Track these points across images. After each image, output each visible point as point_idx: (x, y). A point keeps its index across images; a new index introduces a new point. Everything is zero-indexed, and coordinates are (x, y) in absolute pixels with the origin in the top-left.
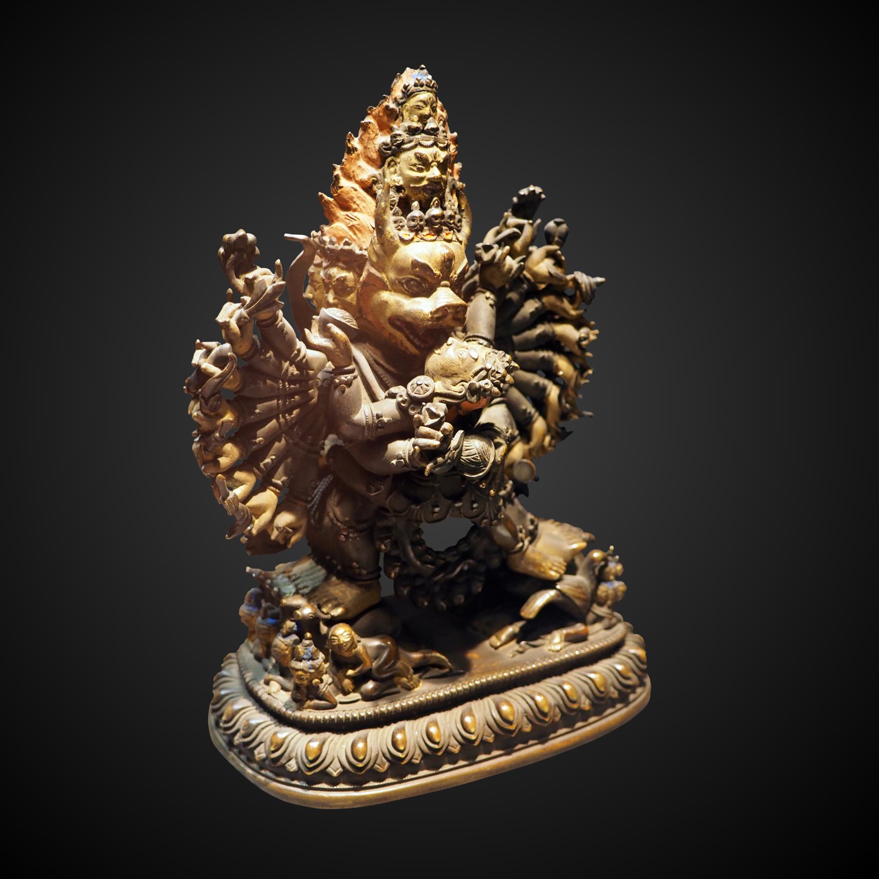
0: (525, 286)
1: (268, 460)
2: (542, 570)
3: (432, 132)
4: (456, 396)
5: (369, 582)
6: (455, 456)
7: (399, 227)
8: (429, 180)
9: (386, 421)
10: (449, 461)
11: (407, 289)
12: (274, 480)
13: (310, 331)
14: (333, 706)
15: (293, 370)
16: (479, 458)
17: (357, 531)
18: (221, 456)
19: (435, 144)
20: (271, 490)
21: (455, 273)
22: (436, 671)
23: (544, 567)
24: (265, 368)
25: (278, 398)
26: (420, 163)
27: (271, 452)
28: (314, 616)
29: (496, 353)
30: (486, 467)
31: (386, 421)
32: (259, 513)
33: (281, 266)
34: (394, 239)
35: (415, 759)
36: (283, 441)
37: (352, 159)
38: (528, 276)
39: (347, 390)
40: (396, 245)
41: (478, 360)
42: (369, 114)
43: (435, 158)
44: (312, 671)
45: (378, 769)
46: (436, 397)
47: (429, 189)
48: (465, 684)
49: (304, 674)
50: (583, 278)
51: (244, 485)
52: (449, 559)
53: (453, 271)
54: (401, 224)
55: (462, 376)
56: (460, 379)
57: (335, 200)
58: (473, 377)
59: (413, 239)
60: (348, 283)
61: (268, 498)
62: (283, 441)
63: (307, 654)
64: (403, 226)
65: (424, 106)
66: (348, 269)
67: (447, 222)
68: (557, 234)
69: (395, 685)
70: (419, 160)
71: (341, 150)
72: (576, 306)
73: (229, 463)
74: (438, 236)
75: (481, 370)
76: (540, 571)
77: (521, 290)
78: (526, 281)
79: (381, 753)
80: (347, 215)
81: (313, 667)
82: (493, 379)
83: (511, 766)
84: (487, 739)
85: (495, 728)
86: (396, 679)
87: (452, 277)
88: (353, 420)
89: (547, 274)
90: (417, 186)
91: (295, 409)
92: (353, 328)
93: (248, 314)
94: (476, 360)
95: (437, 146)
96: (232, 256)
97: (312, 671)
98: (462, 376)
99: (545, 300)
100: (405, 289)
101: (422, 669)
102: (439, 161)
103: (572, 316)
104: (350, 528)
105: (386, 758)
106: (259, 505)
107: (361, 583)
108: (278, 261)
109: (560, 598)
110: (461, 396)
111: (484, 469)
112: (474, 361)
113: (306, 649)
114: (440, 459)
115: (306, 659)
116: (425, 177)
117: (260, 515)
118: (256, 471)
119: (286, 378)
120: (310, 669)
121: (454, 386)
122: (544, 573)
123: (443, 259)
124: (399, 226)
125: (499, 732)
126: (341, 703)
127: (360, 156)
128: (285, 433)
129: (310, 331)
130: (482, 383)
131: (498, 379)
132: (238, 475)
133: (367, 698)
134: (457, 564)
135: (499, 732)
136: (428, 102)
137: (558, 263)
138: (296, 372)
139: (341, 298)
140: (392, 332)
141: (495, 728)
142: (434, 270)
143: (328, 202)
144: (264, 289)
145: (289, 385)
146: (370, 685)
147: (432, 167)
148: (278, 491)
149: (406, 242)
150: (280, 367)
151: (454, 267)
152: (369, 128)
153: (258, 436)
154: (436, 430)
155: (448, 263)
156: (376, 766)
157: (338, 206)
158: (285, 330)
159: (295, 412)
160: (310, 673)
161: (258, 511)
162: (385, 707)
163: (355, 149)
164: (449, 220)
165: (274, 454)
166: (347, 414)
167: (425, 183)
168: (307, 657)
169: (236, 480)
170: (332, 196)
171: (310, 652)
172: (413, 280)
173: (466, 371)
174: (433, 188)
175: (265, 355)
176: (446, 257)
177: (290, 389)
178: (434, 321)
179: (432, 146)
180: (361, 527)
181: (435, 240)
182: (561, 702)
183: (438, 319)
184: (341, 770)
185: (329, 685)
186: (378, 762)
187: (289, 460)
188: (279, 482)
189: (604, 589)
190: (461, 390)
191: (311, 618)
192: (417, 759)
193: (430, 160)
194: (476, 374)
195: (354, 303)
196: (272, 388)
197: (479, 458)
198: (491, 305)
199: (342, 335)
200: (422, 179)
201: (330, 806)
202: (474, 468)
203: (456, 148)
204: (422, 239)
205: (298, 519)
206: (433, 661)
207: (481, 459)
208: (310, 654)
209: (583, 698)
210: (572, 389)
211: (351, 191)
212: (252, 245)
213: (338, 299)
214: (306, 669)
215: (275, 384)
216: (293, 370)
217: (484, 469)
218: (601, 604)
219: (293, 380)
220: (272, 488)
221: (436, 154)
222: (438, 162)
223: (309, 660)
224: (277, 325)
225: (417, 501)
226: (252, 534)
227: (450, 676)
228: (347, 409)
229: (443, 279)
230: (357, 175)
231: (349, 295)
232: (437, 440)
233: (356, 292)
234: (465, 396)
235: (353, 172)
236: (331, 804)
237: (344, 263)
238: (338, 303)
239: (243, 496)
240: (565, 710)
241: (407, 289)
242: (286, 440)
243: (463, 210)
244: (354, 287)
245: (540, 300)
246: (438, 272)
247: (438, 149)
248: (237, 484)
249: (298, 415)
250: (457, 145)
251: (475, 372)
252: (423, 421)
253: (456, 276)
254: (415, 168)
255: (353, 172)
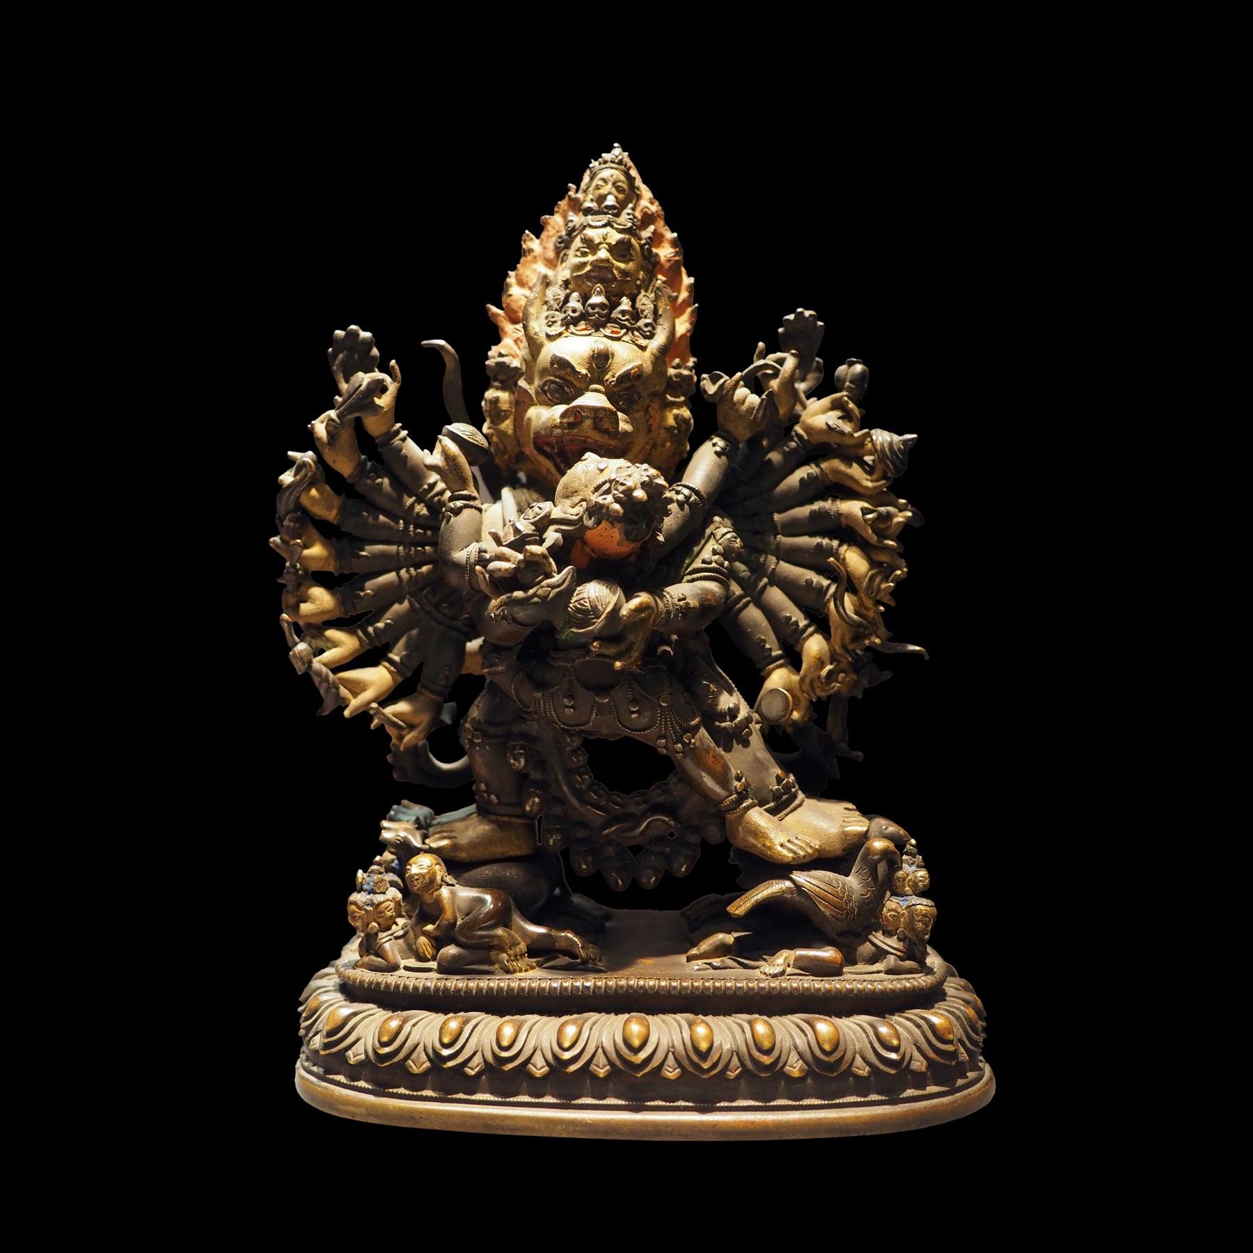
0: (793, 444)
1: (380, 625)
2: (768, 844)
3: (606, 210)
4: (571, 520)
5: (506, 819)
6: (551, 596)
7: (550, 323)
8: (592, 263)
9: (488, 558)
10: (536, 599)
11: (551, 398)
12: (391, 655)
13: (432, 454)
14: (394, 968)
15: (421, 509)
16: (588, 604)
17: (485, 735)
18: (305, 602)
19: (609, 224)
20: (385, 667)
21: (613, 376)
22: (564, 960)
23: (771, 840)
24: (381, 501)
25: (399, 544)
26: (585, 245)
27: (388, 615)
28: (402, 841)
29: (638, 467)
30: (598, 618)
31: (488, 558)
32: (359, 692)
33: (379, 360)
34: (538, 336)
35: (468, 1067)
36: (406, 603)
37: (526, 262)
38: (801, 432)
39: (452, 519)
40: (541, 343)
41: (604, 472)
42: (557, 212)
43: (605, 239)
44: (369, 908)
45: (411, 1067)
46: (552, 525)
47: (594, 277)
48: (587, 981)
49: (357, 910)
50: (881, 437)
51: (338, 648)
52: (632, 809)
53: (610, 373)
54: (552, 320)
55: (582, 493)
56: (579, 498)
57: (506, 313)
58: (593, 494)
59: (560, 334)
60: (501, 405)
61: (377, 677)
62: (406, 603)
63: (368, 884)
64: (556, 322)
65: (604, 184)
66: (503, 389)
67: (617, 318)
68: (849, 377)
69: (492, 963)
70: (584, 243)
71: (513, 256)
72: (875, 477)
73: (314, 611)
74: (596, 331)
75: (604, 483)
76: (764, 845)
77: (787, 449)
78: (796, 439)
79: (421, 1046)
80: (516, 329)
81: (372, 904)
82: (616, 492)
83: (632, 1133)
84: (595, 1070)
85: (613, 1056)
86: (493, 954)
87: (607, 380)
88: (453, 557)
89: (824, 426)
90: (579, 273)
91: (426, 564)
92: (469, 442)
93: (338, 416)
94: (602, 471)
95: (612, 227)
96: (341, 356)
97: (369, 908)
98: (582, 493)
99: (824, 465)
100: (549, 399)
101: (541, 952)
102: (610, 243)
103: (867, 488)
104: (476, 730)
105: (427, 1055)
106: (357, 679)
107: (494, 817)
108: (393, 362)
109: (796, 897)
110: (576, 520)
111: (595, 620)
112: (598, 472)
113: (369, 876)
114: (518, 594)
115: (366, 890)
116: (588, 261)
117: (359, 694)
118: (360, 633)
119: (408, 515)
120: (368, 905)
121: (573, 507)
122: (770, 848)
123: (591, 354)
124: (549, 321)
125: (618, 1063)
126: (407, 968)
127: (538, 258)
128: (411, 595)
129: (432, 454)
130: (600, 500)
131: (621, 493)
132: (332, 633)
133: (447, 969)
134: (644, 816)
135: (618, 1063)
136: (609, 180)
137: (847, 416)
138: (425, 511)
139: (496, 427)
140: (549, 468)
141: (613, 1056)
142: (576, 366)
143: (499, 315)
144: (357, 385)
145: (415, 528)
146: (451, 950)
147: (600, 250)
148: (392, 668)
149: (550, 338)
150: (400, 501)
151: (612, 368)
152: (549, 224)
153: (366, 588)
154: (516, 551)
155: (601, 360)
156: (410, 1062)
157: (508, 319)
158: (404, 451)
159: (424, 569)
160: (366, 910)
161: (356, 687)
162: (455, 983)
163: (531, 251)
164: (620, 316)
165: (390, 617)
166: (447, 549)
167: (588, 268)
168: (367, 888)
169: (328, 640)
170: (502, 308)
171: (372, 881)
172: (553, 382)
173: (586, 487)
174: (599, 276)
175: (374, 480)
176: (596, 351)
177: (416, 534)
178: (565, 429)
179: (604, 226)
180: (493, 730)
181: (590, 335)
182: (744, 1049)
183: (571, 426)
184: (363, 1057)
185: (396, 938)
186: (413, 1056)
187: (415, 632)
188: (397, 659)
189: (892, 904)
190: (578, 512)
191: (398, 842)
192: (472, 1069)
193: (597, 241)
194: (597, 489)
195: (510, 432)
196: (384, 526)
197: (588, 604)
198: (716, 453)
199: (456, 454)
200: (584, 264)
201: (337, 1110)
202: (581, 619)
203: (676, 252)
204: (572, 333)
205: (415, 712)
206: (562, 945)
207: (591, 606)
208: (372, 883)
209: (794, 1057)
210: (863, 592)
211: (521, 299)
212: (367, 345)
213: (494, 429)
214: (360, 904)
215: (392, 524)
216: (421, 509)
217: (595, 620)
218: (888, 933)
219: (419, 522)
220: (386, 664)
221: (606, 235)
222: (609, 244)
223: (369, 894)
224: (393, 443)
225: (541, 685)
226: (399, 750)
227: (580, 970)
228: (448, 543)
229: (592, 382)
230: (531, 280)
231: (503, 421)
232: (514, 563)
233: (512, 417)
234: (581, 519)
235: (527, 277)
236: (340, 1107)
237: (501, 382)
238: (492, 434)
239: (332, 659)
240: (749, 1064)
241: (551, 398)
242: (410, 602)
243: (660, 315)
244: (509, 411)
245: (818, 466)
246: (584, 371)
247: (614, 231)
248: (329, 645)
249: (430, 572)
250: (677, 249)
251: (596, 486)
252: (502, 539)
253: (615, 379)
254: (579, 254)
255: (527, 277)
